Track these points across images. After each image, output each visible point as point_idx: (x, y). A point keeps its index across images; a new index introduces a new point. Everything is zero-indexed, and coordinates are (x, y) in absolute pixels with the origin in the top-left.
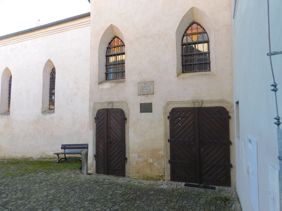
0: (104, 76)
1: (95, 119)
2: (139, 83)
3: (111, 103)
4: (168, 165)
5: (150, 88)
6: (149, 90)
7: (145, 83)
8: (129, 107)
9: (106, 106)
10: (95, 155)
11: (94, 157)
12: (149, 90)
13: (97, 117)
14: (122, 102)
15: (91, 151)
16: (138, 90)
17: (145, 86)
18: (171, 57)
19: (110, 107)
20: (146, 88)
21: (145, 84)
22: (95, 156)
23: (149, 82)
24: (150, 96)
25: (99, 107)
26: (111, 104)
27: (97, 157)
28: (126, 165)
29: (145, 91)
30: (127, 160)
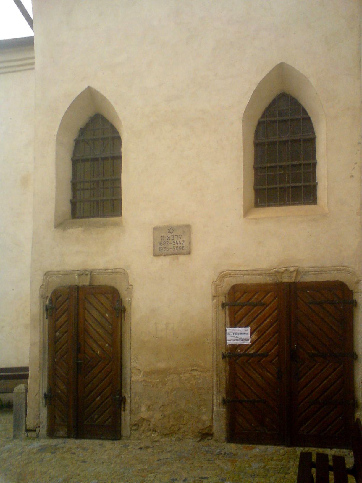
0: (67, 208)
1: (47, 310)
2: (155, 229)
3: (91, 273)
4: (222, 410)
5: (181, 240)
6: (179, 245)
7: (171, 229)
8: (131, 284)
9: (76, 281)
10: (45, 394)
11: (44, 399)
12: (179, 245)
13: (51, 305)
14: (115, 272)
15: (36, 388)
16: (154, 244)
17: (170, 235)
18: (226, 163)
19: (86, 282)
20: (172, 242)
21: (171, 231)
22: (46, 397)
23: (180, 227)
24: (182, 258)
25: (56, 282)
26: (87, 275)
27: (50, 398)
28: (123, 413)
29: (171, 246)
30: (125, 403)
